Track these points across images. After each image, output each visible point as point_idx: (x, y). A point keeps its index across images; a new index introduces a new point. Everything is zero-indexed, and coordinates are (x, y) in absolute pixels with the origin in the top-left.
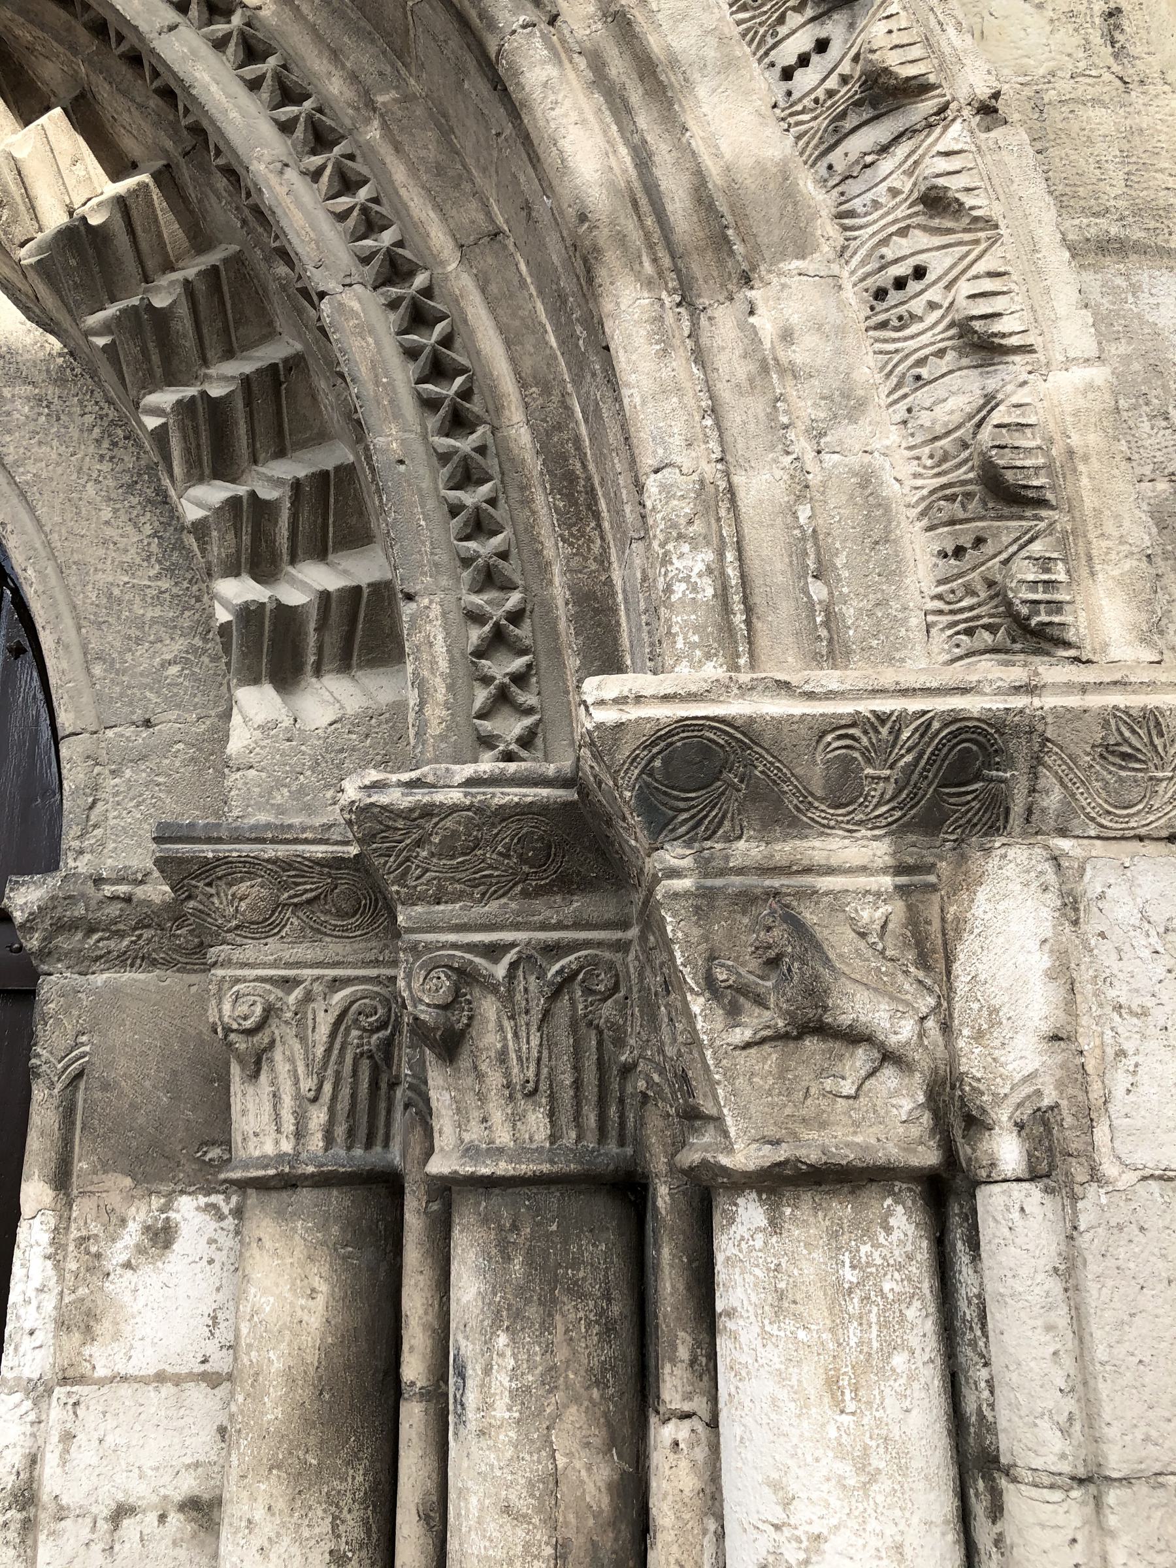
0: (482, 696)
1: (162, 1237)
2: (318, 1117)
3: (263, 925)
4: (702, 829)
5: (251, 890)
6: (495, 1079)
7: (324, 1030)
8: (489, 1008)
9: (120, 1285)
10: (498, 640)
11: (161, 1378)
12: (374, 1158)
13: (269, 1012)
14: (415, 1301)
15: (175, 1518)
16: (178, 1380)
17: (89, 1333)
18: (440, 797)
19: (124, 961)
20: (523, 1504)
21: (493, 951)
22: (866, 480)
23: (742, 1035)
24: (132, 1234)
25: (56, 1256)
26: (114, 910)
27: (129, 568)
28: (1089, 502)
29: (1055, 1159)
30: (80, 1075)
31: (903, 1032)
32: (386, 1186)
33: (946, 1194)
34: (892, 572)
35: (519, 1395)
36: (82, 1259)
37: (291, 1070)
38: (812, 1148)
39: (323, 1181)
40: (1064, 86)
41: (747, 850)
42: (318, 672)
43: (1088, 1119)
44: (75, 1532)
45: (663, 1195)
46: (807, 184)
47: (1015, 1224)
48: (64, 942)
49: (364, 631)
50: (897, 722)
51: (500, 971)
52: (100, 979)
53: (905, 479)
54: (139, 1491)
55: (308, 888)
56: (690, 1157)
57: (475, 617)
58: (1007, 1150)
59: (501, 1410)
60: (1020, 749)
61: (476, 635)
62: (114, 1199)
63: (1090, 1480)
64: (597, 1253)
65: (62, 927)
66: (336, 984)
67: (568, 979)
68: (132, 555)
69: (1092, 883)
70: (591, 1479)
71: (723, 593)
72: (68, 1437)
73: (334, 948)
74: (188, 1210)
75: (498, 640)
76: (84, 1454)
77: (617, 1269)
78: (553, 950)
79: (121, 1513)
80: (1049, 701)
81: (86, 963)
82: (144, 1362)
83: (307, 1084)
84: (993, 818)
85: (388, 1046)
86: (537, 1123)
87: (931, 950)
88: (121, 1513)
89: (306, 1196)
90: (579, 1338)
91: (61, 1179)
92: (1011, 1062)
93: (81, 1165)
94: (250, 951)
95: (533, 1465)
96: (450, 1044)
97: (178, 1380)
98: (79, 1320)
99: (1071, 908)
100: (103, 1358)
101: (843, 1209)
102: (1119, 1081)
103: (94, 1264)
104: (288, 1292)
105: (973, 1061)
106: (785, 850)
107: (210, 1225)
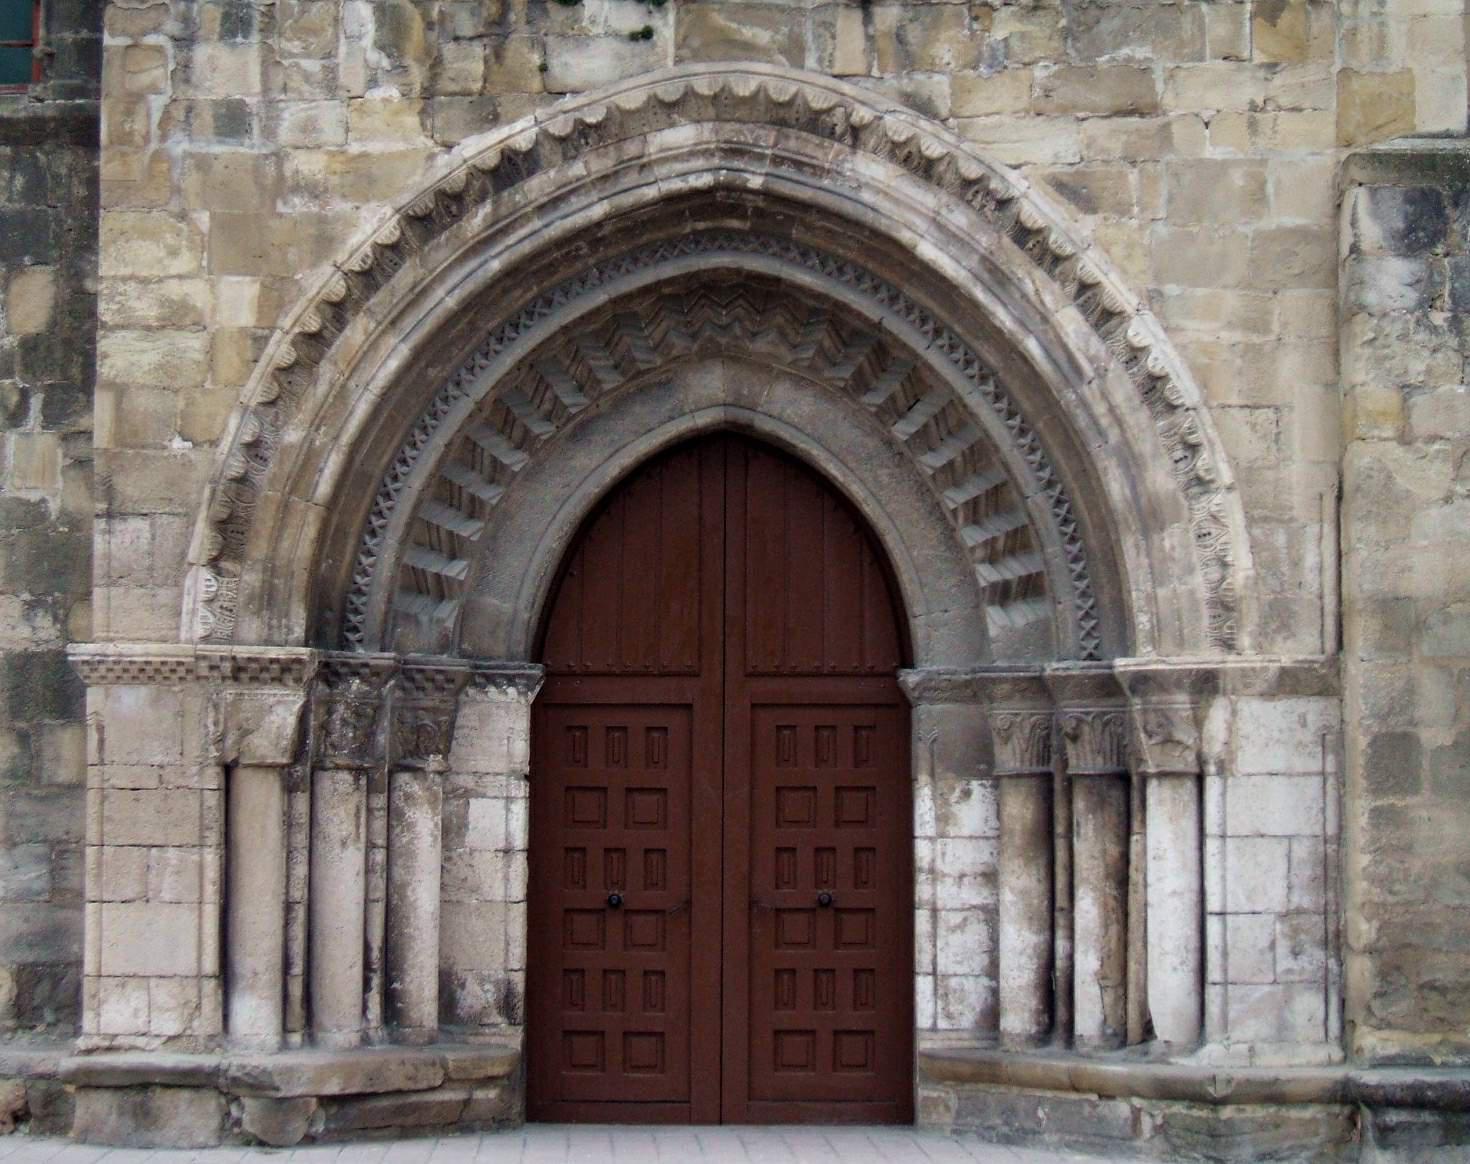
0: (1083, 633)
1: (967, 794)
2: (1027, 756)
3: (1008, 697)
4: (1143, 695)
5: (1006, 687)
6: (1088, 748)
7: (1027, 731)
8: (1086, 729)
9: (955, 808)
10: (1087, 616)
11: (971, 837)
12: (1044, 769)
13: (1012, 724)
14: (1060, 813)
15: (979, 879)
16: (976, 838)
17: (947, 823)
18: (1074, 673)
19: (946, 700)
20: (1097, 855)
21: (1088, 713)
22: (1192, 593)
23: (1153, 741)
24: (957, 793)
25: (934, 799)
26: (944, 684)
27: (932, 547)
28: (1245, 611)
29: (1223, 770)
30: (935, 740)
31: (1190, 742)
32: (1048, 777)
33: (1200, 779)
34: (1198, 619)
35: (1095, 830)
36: (940, 799)
37: (1018, 742)
38: (1167, 769)
39: (1031, 775)
40: (1259, 463)
41: (1154, 699)
42: (1015, 599)
43: (1232, 761)
44: (949, 881)
45: (1135, 779)
46: (1181, 496)
47: (1213, 785)
48: (926, 694)
49: (1031, 587)
50: (1191, 670)
51: (1090, 718)
52: (939, 707)
53: (1203, 594)
54: (968, 870)
55: (1024, 685)
56: (1141, 769)
57: (1079, 608)
58: (1212, 768)
59: (1091, 833)
60: (1222, 676)
61: (1081, 613)
62: (951, 782)
63: (1223, 837)
64: (1116, 794)
65: (925, 689)
66: (1032, 715)
67: (1109, 721)
68: (934, 542)
69: (1240, 705)
70: (1114, 850)
71: (1152, 627)
72: (944, 854)
73: (1029, 704)
74: (975, 785)
75: (1087, 616)
76: (948, 858)
77: (1121, 801)
78: (1105, 713)
79: (962, 876)
80: (1229, 665)
81: (932, 701)
82: (966, 832)
83: (1024, 746)
84: (1215, 691)
85: (1048, 736)
86: (1100, 760)
87: (1198, 722)
88: (962, 876)
89: (1023, 781)
90: (1111, 816)
91: (932, 775)
92: (1214, 748)
93: (938, 770)
94: (1004, 705)
95: (1099, 847)
96: (1075, 738)
97: (976, 838)
98: (943, 818)
99: (1234, 713)
100: (952, 831)
101: (1176, 782)
102: (1240, 754)
103: (946, 803)
104: (1021, 808)
105: (1206, 749)
106: (1166, 697)
107: (983, 791)
